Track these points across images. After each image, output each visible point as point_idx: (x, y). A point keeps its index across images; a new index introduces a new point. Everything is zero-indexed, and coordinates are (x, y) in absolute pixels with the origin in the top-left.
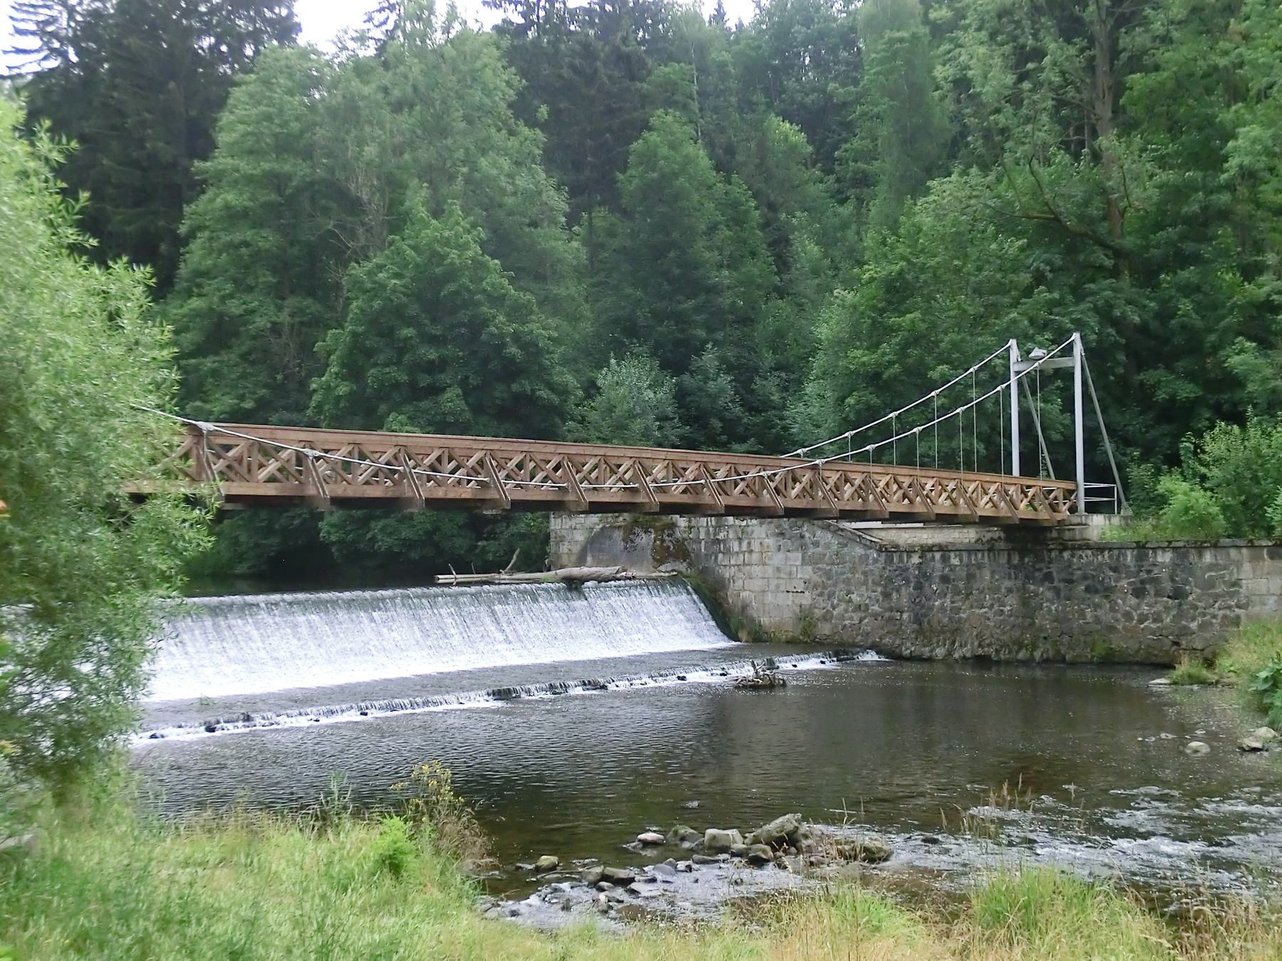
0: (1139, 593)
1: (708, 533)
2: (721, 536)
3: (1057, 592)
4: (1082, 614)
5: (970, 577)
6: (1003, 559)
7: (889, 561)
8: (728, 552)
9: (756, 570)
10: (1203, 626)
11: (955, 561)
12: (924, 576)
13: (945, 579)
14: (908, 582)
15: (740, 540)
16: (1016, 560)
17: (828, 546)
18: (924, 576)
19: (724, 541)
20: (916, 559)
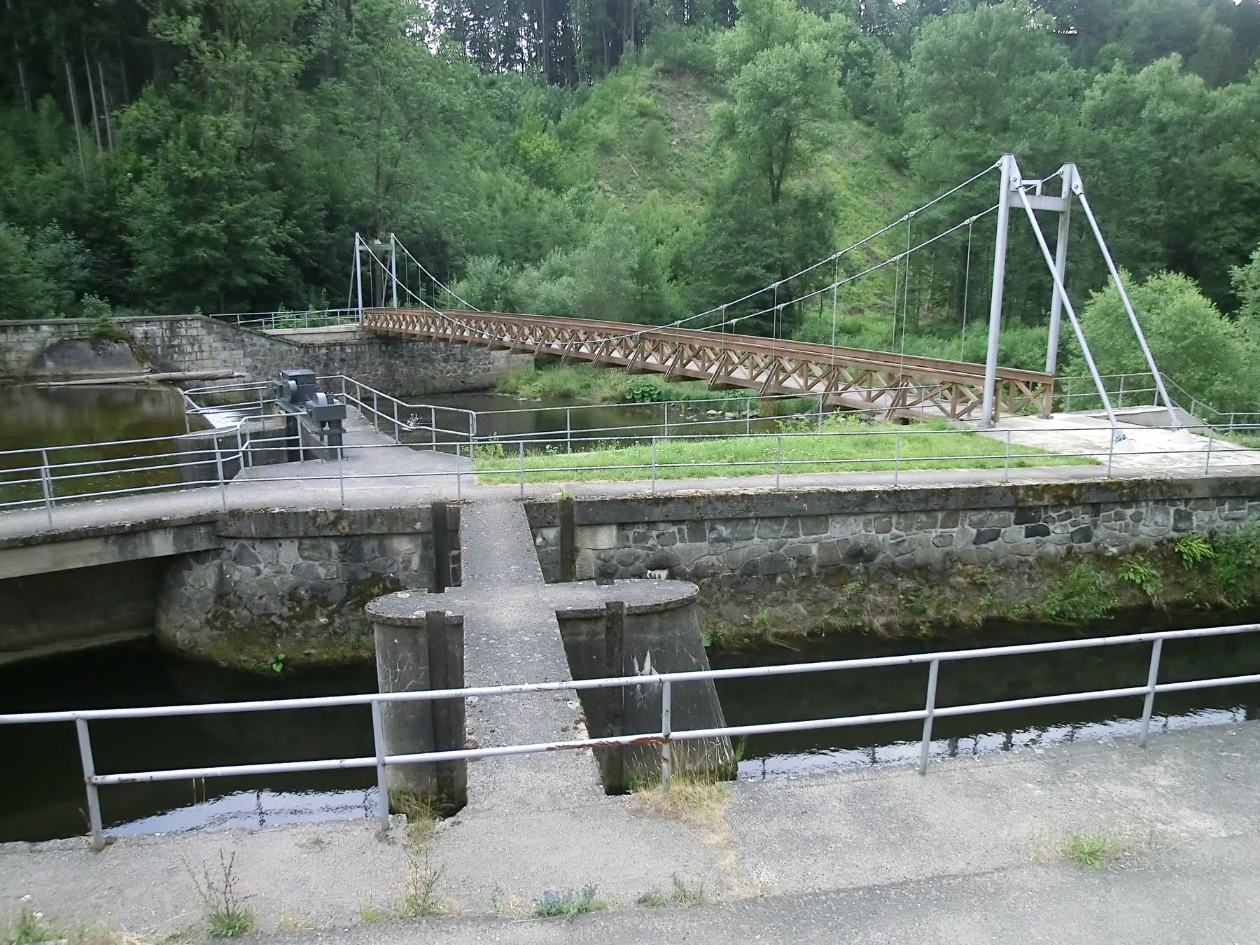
0: (446, 360)
1: (163, 341)
2: (176, 342)
3: (406, 363)
4: (417, 372)
5: (358, 358)
6: (377, 348)
7: (307, 352)
8: (182, 352)
9: (208, 362)
10: (476, 373)
11: (349, 350)
12: (330, 359)
13: (342, 360)
14: (319, 363)
15: (192, 345)
16: (384, 348)
17: (262, 346)
18: (330, 359)
19: (179, 346)
20: (324, 351)
